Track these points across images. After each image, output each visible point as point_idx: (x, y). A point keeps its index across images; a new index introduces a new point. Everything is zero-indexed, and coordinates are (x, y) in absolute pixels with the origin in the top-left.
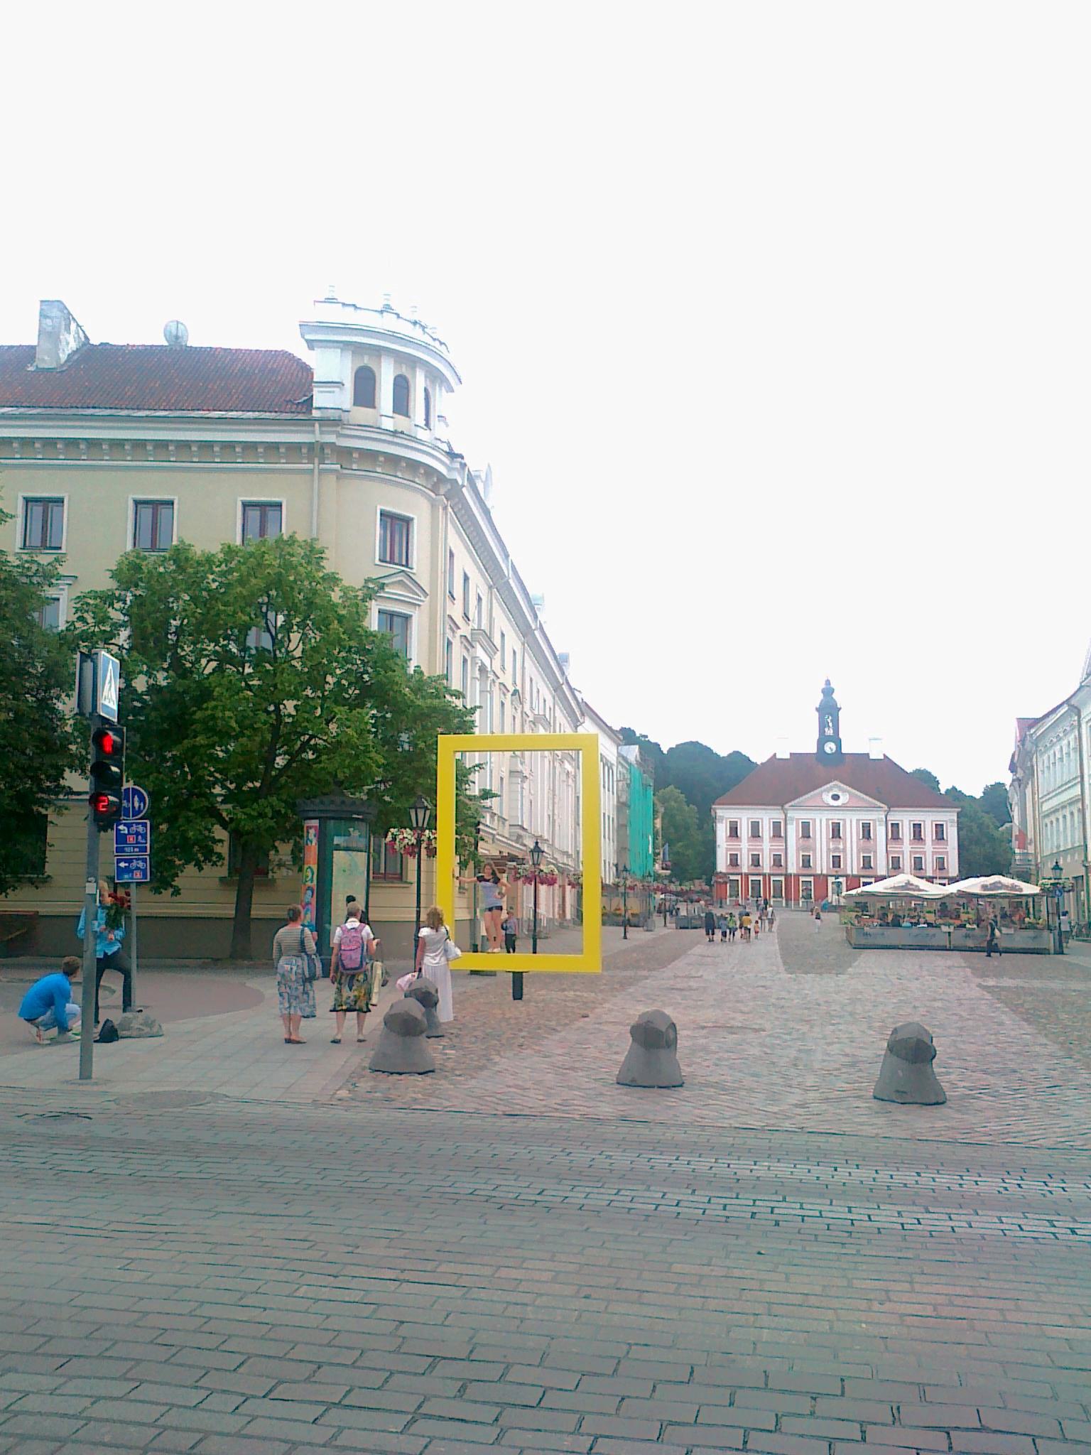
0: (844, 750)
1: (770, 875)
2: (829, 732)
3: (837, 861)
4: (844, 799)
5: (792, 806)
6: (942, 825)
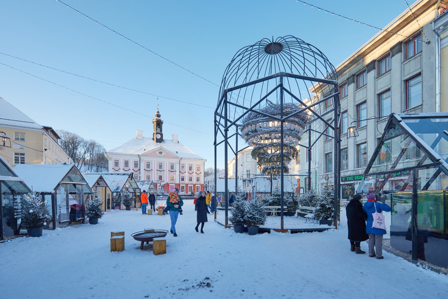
3: (160, 178)
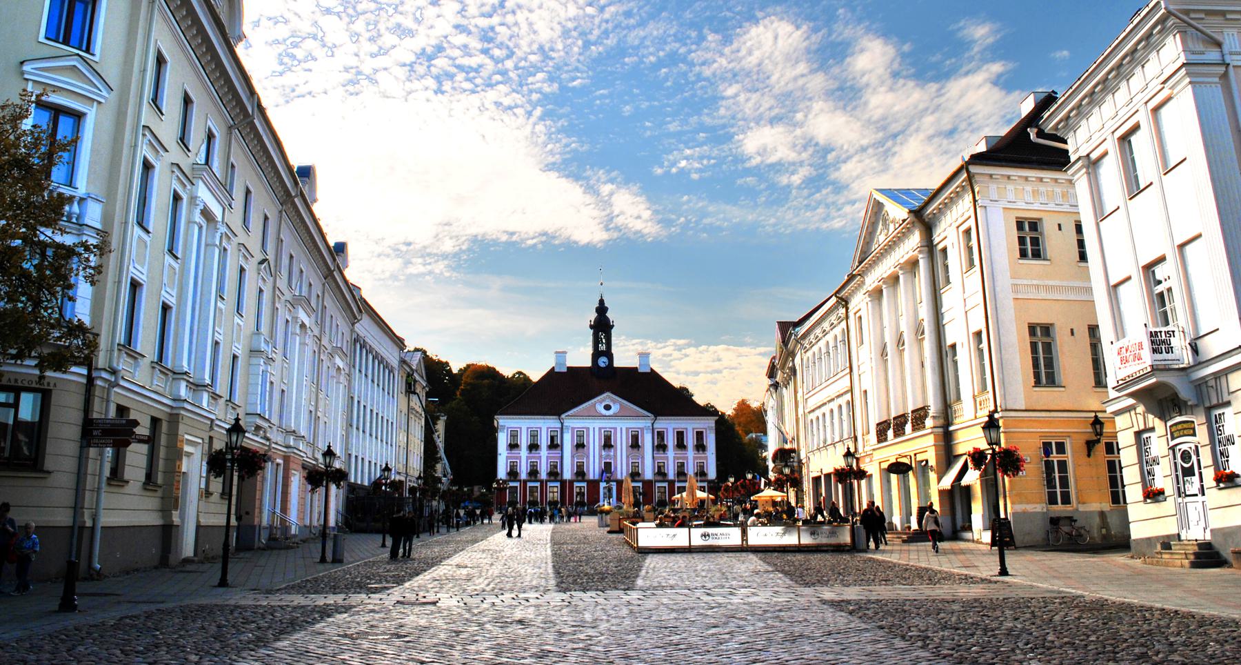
0: (615, 365)
1: (547, 481)
2: (602, 347)
4: (615, 409)
5: (568, 416)
6: (702, 432)
